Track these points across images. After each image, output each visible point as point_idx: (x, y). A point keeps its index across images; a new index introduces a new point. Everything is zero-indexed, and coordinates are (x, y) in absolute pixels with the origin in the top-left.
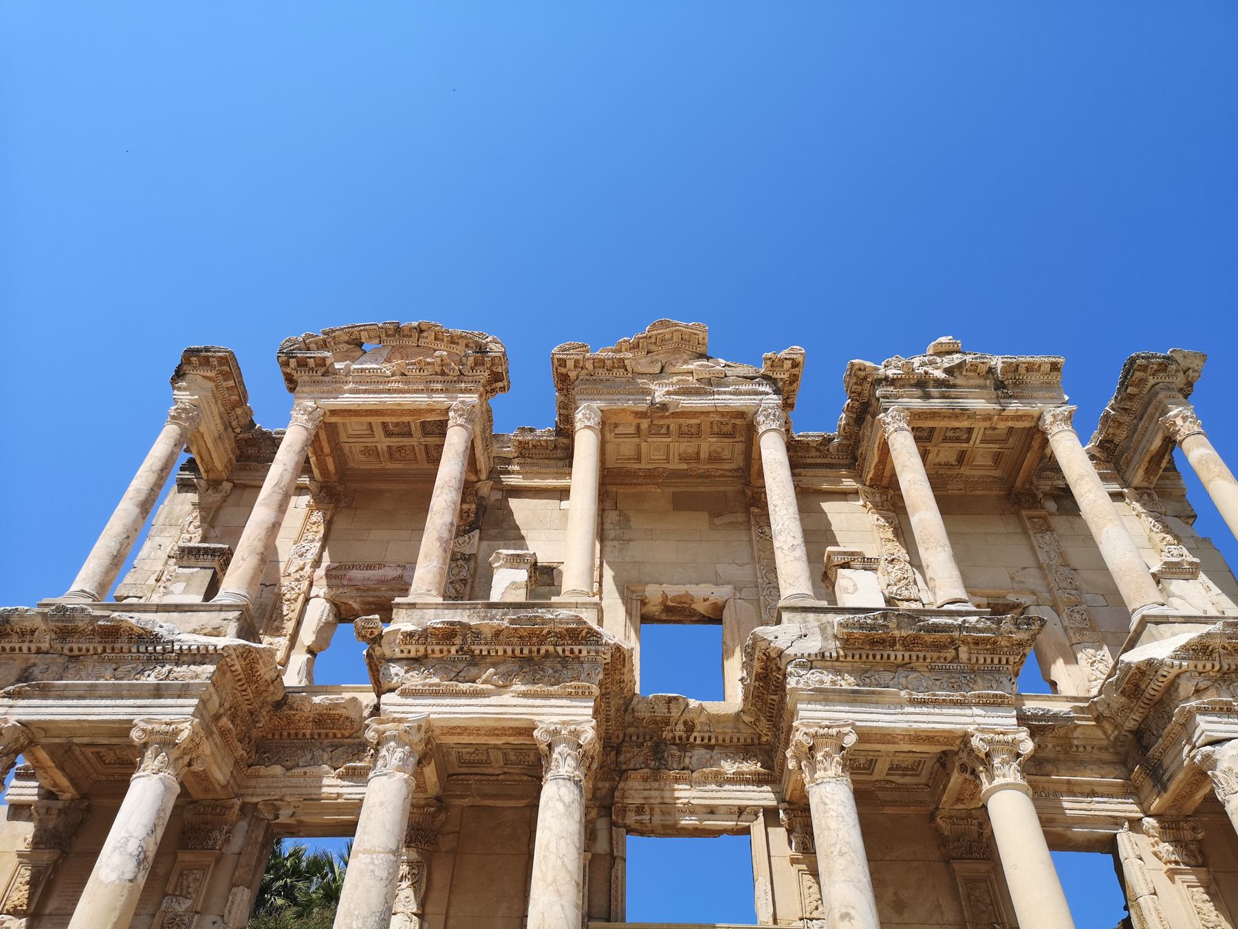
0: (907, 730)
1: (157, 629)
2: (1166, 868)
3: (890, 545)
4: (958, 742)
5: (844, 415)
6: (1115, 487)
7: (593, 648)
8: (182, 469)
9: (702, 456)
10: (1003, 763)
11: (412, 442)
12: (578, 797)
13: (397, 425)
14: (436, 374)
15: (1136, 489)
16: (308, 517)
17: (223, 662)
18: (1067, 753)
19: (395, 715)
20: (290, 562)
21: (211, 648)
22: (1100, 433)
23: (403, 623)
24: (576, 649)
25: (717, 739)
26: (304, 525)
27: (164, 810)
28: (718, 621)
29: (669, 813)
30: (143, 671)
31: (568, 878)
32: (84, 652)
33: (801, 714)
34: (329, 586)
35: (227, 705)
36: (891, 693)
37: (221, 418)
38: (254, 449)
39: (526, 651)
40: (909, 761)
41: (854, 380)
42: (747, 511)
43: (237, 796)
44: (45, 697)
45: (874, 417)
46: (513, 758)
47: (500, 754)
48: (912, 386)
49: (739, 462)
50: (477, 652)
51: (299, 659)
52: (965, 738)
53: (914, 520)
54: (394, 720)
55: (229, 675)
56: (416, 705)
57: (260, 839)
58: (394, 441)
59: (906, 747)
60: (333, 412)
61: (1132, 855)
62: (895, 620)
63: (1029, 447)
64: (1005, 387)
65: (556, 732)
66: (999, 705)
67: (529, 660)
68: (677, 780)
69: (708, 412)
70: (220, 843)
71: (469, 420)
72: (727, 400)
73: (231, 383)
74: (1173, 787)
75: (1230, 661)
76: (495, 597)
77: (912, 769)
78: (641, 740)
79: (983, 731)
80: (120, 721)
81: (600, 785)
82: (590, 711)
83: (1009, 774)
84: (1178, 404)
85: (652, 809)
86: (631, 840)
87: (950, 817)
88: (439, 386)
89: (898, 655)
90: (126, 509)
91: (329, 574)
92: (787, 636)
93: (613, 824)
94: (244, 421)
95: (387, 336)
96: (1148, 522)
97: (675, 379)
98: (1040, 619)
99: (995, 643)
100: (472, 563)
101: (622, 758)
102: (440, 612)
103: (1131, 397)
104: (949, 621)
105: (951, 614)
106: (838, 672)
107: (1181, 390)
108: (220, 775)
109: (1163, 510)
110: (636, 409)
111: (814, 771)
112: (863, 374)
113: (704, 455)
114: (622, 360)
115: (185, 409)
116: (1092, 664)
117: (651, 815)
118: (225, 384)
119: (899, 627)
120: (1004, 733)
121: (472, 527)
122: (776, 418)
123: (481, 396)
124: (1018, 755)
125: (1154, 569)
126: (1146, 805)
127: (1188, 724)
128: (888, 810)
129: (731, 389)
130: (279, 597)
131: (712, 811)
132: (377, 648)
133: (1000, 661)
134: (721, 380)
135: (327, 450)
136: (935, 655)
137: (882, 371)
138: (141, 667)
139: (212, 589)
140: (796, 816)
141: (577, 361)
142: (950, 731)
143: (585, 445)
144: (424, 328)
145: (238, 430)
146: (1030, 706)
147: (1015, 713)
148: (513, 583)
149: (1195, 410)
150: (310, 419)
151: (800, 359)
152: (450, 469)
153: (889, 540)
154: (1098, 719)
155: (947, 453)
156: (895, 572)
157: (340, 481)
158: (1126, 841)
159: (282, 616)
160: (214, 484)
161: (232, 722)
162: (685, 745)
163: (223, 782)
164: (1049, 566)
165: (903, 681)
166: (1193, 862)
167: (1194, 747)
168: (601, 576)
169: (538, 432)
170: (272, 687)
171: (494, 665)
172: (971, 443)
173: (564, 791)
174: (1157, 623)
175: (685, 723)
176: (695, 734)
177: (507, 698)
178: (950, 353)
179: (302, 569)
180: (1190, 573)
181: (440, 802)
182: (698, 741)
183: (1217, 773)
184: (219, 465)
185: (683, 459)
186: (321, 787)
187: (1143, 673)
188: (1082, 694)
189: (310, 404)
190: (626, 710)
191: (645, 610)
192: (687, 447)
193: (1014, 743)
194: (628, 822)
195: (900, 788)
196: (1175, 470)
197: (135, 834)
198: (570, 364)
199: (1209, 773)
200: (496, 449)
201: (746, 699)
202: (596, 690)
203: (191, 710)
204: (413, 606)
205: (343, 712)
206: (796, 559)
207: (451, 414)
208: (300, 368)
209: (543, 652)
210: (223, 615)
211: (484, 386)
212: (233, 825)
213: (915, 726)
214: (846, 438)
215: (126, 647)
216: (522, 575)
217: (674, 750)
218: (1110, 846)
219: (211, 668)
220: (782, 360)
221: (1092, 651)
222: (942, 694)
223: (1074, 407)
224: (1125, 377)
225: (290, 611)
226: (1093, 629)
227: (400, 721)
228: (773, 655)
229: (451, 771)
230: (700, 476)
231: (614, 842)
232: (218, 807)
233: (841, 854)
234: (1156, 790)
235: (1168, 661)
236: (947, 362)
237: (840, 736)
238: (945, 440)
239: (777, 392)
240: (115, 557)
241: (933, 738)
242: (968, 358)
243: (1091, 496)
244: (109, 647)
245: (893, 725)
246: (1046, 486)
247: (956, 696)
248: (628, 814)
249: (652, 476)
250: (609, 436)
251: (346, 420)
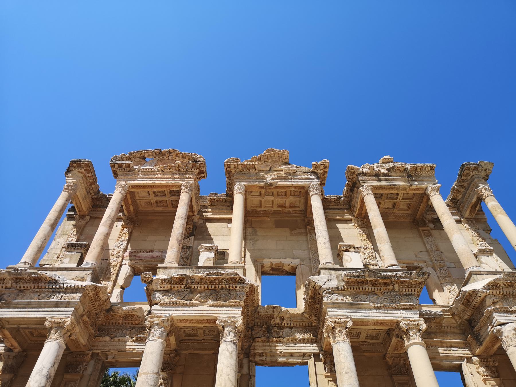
0: (373, 320)
1: (57, 278)
2: (482, 378)
3: (365, 242)
4: (395, 325)
5: (345, 188)
6: (458, 218)
7: (241, 285)
8: (69, 211)
9: (287, 205)
10: (414, 333)
11: (166, 199)
12: (235, 349)
13: (160, 192)
14: (176, 171)
16: (122, 231)
17: (85, 292)
18: (440, 329)
19: (158, 315)
20: (114, 250)
21: (80, 286)
22: (451, 196)
23: (161, 275)
24: (234, 286)
25: (294, 324)
26: (120, 234)
27: (58, 356)
28: (294, 274)
29: (274, 356)
30: (51, 296)
31: (231, 384)
32: (26, 288)
33: (329, 313)
34: (130, 260)
35: (86, 311)
36: (366, 304)
37: (86, 189)
38: (100, 202)
39: (213, 287)
40: (374, 333)
41: (349, 173)
42: (306, 228)
43: (90, 350)
44: (9, 307)
45: (358, 188)
46: (207, 333)
47: (202, 331)
48: (373, 176)
49: (302, 207)
50: (193, 287)
51: (117, 291)
52: (398, 323)
53: (375, 232)
54: (157, 317)
55: (87, 297)
56: (167, 310)
57: (100, 368)
58: (159, 199)
59: (373, 327)
60: (133, 187)
61: (468, 373)
62: (367, 273)
63: (422, 202)
64: (411, 176)
65: (226, 322)
66: (412, 309)
67: (215, 291)
68: (277, 342)
69: (289, 187)
70: (82, 370)
71: (190, 190)
72: (297, 182)
73: (90, 175)
74: (484, 343)
76: (200, 264)
77: (376, 337)
78: (262, 325)
79: (405, 320)
80: (40, 318)
81: (245, 344)
82: (240, 312)
83: (416, 338)
84: (483, 184)
85: (266, 355)
86: (257, 367)
87: (392, 357)
88: (177, 176)
89: (369, 288)
91: (130, 255)
92: (323, 280)
93: (250, 361)
94: (95, 191)
95: (156, 155)
96: (472, 232)
97: (276, 173)
98: (428, 273)
99: (409, 283)
100: (191, 250)
101: (254, 333)
102: (177, 270)
103: (463, 181)
104: (390, 274)
105: (391, 271)
106: (344, 295)
107: (484, 178)
108: (83, 341)
109: (477, 227)
110: (259, 185)
111: (334, 337)
112: (353, 171)
113: (288, 204)
114: (254, 165)
115: (70, 186)
116: (450, 292)
117: (266, 357)
118: (87, 175)
119: (369, 276)
120: (414, 321)
121: (191, 235)
122: (318, 189)
123: (195, 180)
124: (420, 330)
125: (475, 252)
126: (473, 351)
127: (490, 317)
128: (366, 354)
129: (298, 177)
130: (109, 265)
131: (292, 355)
132: (150, 286)
133: (412, 290)
134: (295, 173)
135: (130, 202)
136: (385, 288)
137: (361, 170)
138: (50, 294)
139: (81, 261)
140: (327, 357)
141: (235, 165)
142: (391, 320)
143: (238, 200)
144: (171, 151)
145: (93, 194)
146: (425, 309)
147: (418, 312)
148: (208, 258)
149: (490, 186)
150: (123, 190)
151: (327, 165)
152: (182, 210)
153: (365, 240)
154: (453, 315)
155: (388, 204)
156: (368, 253)
157: (136, 216)
158: (466, 367)
159: (110, 273)
160: (82, 217)
161: (88, 318)
162: (280, 327)
163: (84, 344)
164: (431, 251)
165: (371, 299)
166: (494, 376)
167: (493, 327)
168: (245, 255)
169: (219, 195)
170: (105, 303)
171: (200, 293)
174: (476, 274)
175: (280, 317)
176: (284, 322)
177: (205, 307)
178: (389, 162)
179: (119, 253)
180: (489, 254)
181: (177, 352)
182: (286, 325)
183: (503, 337)
184: (84, 209)
185: (279, 206)
186: (126, 346)
187: (471, 295)
188: (446, 304)
189: (123, 183)
190: (255, 312)
191: (263, 270)
192: (281, 201)
193: (418, 325)
194: (256, 360)
195: (371, 345)
196: (482, 210)
197: (46, 367)
198: (232, 167)
199: (500, 337)
200: (201, 202)
201: (306, 307)
202: (243, 303)
203: (71, 313)
204: (165, 268)
205: (136, 313)
206: (326, 248)
207: (182, 187)
208: (119, 168)
209: (220, 287)
210: (85, 272)
211: (196, 176)
212: (88, 362)
213: (377, 318)
214: (346, 197)
215: (43, 286)
216: (212, 255)
217: (276, 329)
218: (459, 369)
219: (80, 295)
220: (320, 165)
221: (450, 286)
222: (388, 304)
223: (440, 185)
224: (461, 173)
225: (113, 270)
226: (450, 277)
227: (160, 317)
228: (317, 288)
229: (181, 339)
230: (286, 213)
231: (250, 369)
232: (82, 354)
233: (346, 373)
234: (477, 345)
235: (481, 290)
236: (388, 166)
238: (387, 198)
239: (318, 178)
240: (40, 248)
241: (384, 323)
242: (396, 164)
243: (448, 221)
244: (36, 286)
245: (367, 318)
246: (429, 217)
247: (394, 305)
248: (256, 356)
249: (266, 213)
250: (248, 197)
251: (139, 190)
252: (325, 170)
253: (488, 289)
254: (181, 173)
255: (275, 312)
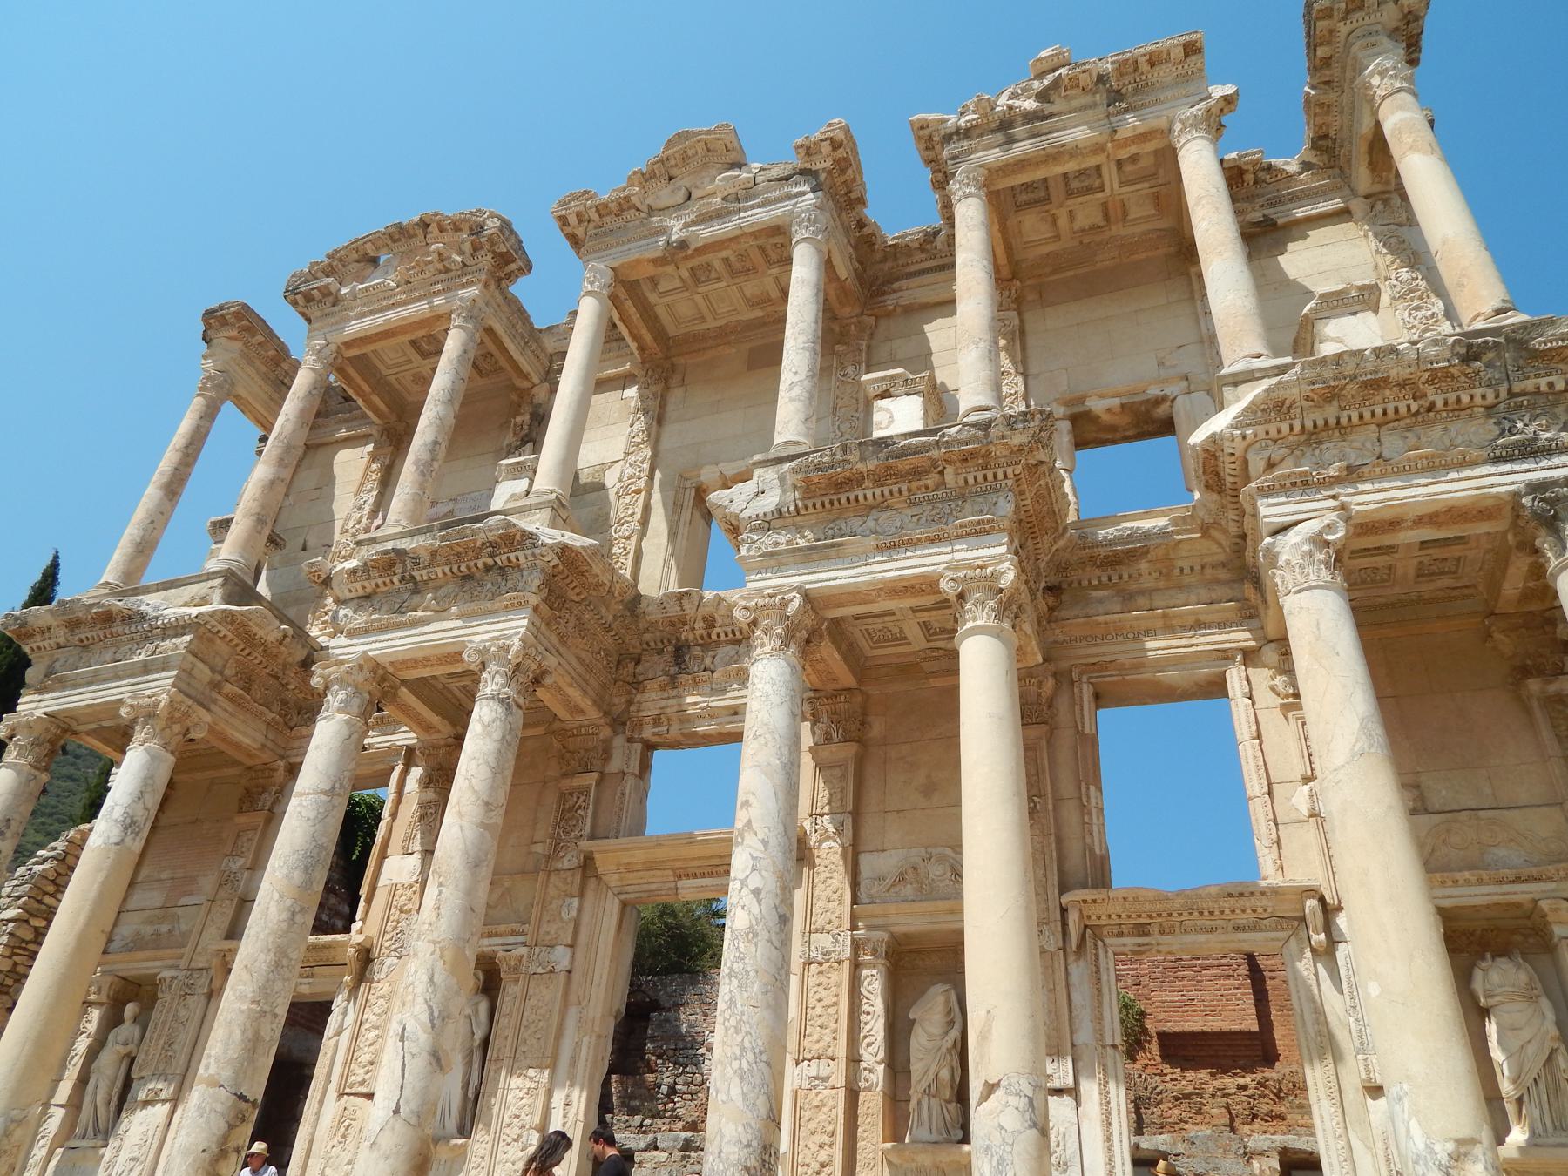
7: (529, 552)
15: (1366, 197)
16: (368, 466)
20: (347, 520)
24: (512, 556)
26: (365, 474)
27: (152, 777)
36: (854, 543)
39: (463, 568)
43: (282, 757)
44: (64, 688)
48: (993, 131)
60: (349, 344)
65: (487, 650)
66: (987, 533)
67: (468, 577)
69: (737, 237)
72: (756, 216)
75: (1312, 416)
81: (616, 700)
89: (869, 492)
90: (151, 493)
92: (743, 497)
101: (640, 668)
103: (1327, 62)
106: (799, 529)
112: (925, 132)
118: (254, 341)
119: (863, 459)
123: (486, 285)
133: (995, 477)
135: (366, 388)
136: (914, 485)
157: (400, 419)
162: (707, 644)
172: (1108, 189)
173: (486, 710)
174: (1236, 384)
175: (704, 619)
176: (717, 630)
182: (723, 637)
193: (995, 576)
198: (573, 220)
206: (791, 400)
210: (211, 583)
213: (879, 576)
217: (697, 651)
237: (784, 604)
238: (1070, 194)
249: (723, 335)
252: (840, 153)
253: (1249, 425)
254: (449, 275)
255: (687, 606)
